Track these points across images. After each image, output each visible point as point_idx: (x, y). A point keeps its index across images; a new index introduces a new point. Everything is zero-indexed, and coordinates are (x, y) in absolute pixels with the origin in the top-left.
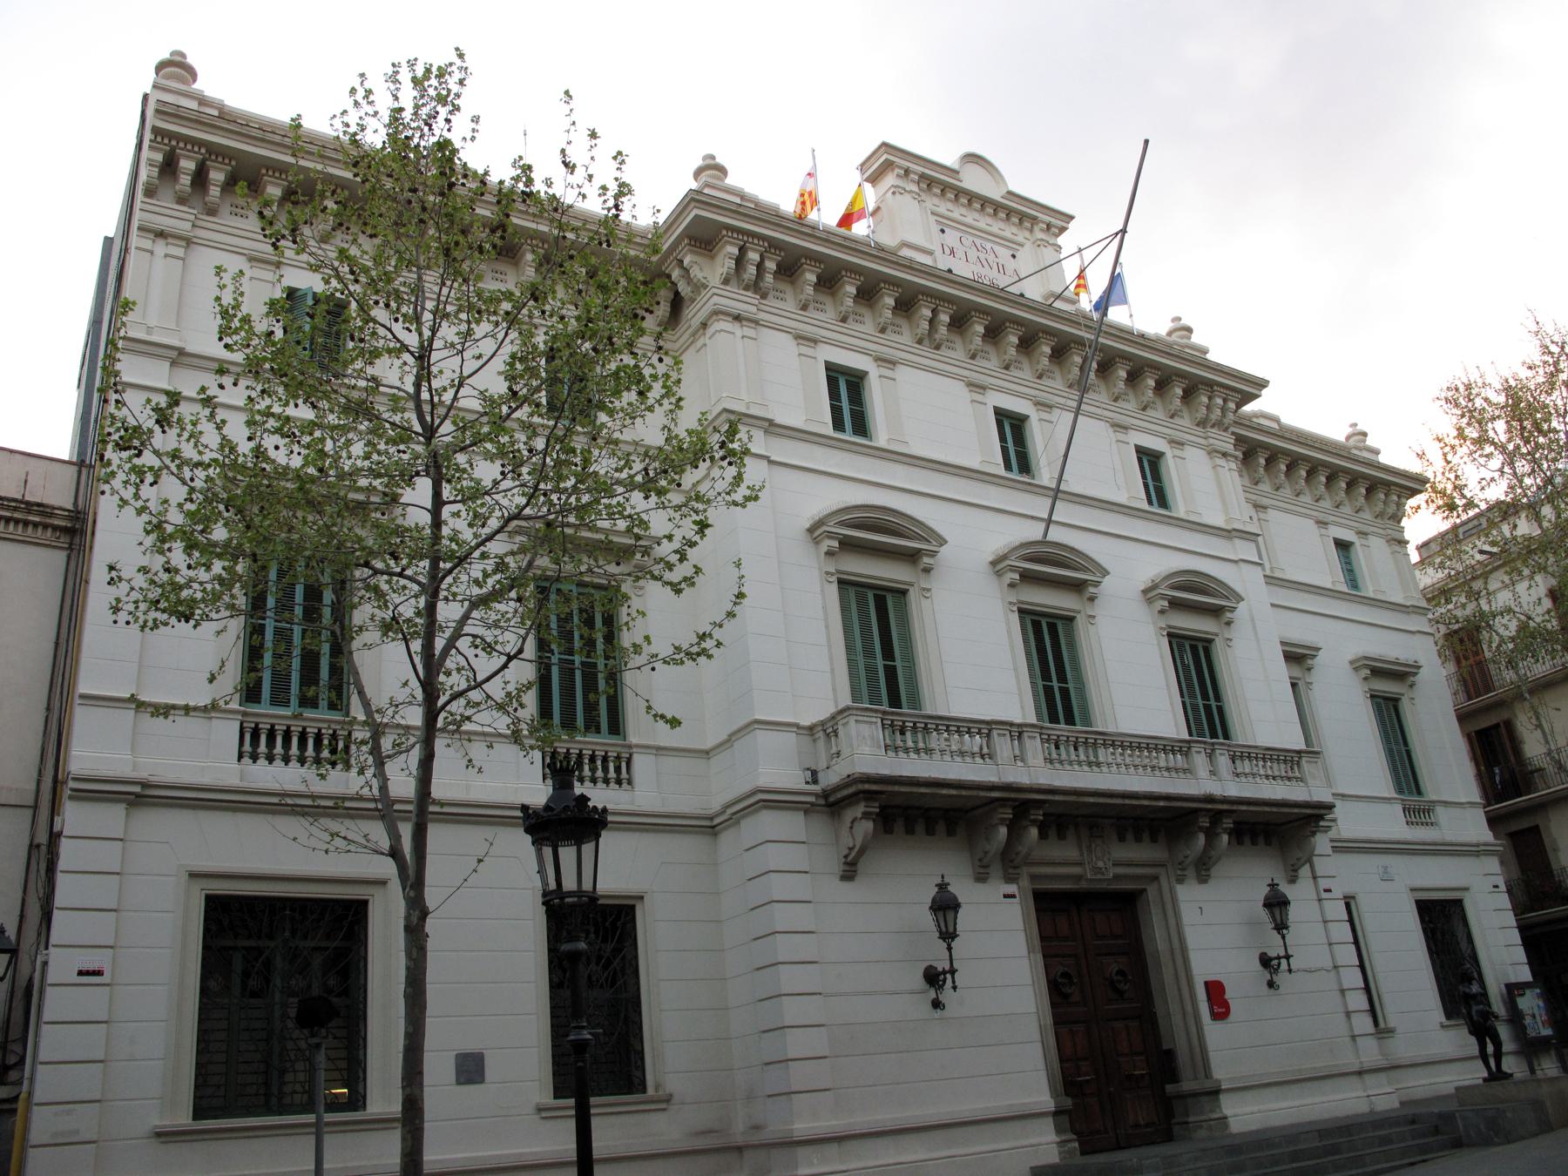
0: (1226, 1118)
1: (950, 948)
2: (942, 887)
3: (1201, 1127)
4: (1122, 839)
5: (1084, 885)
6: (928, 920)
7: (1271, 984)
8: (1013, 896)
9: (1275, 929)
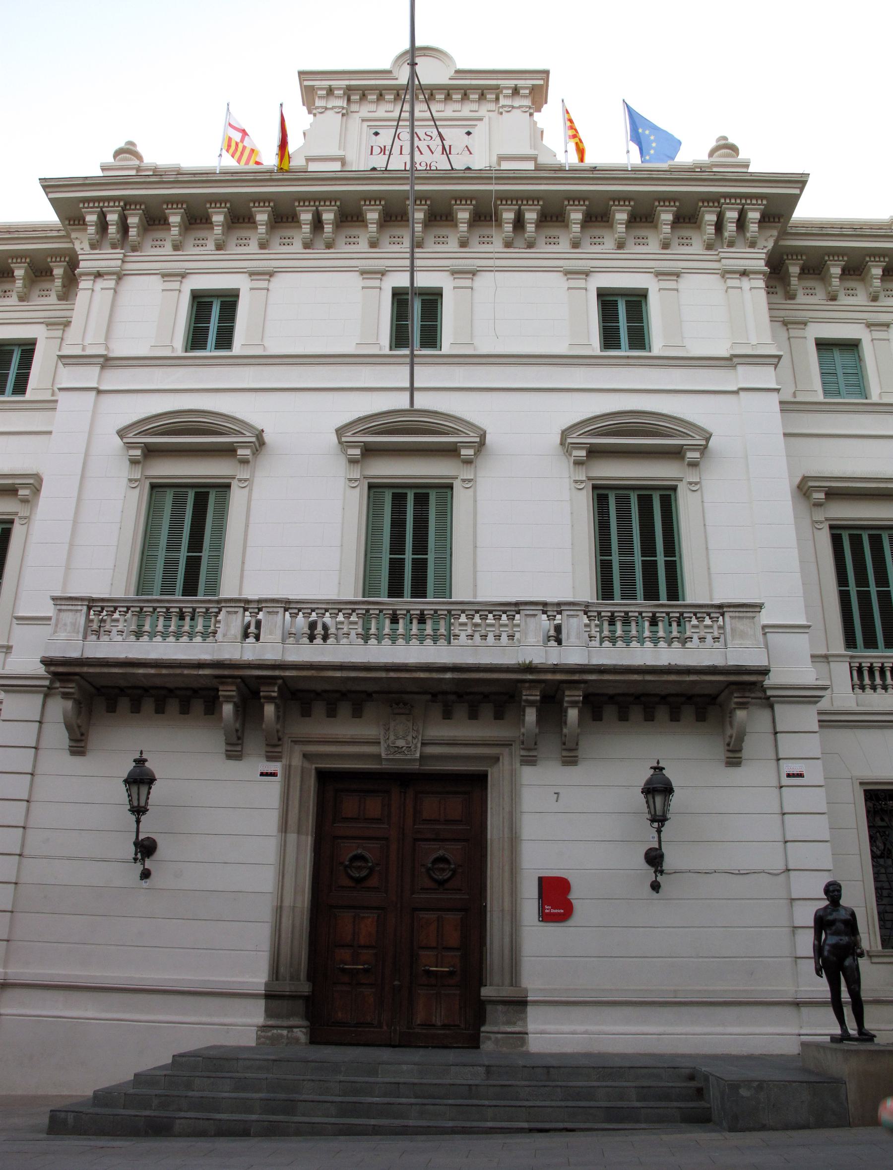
0: (527, 1034)
1: (138, 822)
2: (140, 762)
3: (489, 1038)
4: (447, 715)
5: (385, 766)
7: (656, 887)
8: (274, 775)
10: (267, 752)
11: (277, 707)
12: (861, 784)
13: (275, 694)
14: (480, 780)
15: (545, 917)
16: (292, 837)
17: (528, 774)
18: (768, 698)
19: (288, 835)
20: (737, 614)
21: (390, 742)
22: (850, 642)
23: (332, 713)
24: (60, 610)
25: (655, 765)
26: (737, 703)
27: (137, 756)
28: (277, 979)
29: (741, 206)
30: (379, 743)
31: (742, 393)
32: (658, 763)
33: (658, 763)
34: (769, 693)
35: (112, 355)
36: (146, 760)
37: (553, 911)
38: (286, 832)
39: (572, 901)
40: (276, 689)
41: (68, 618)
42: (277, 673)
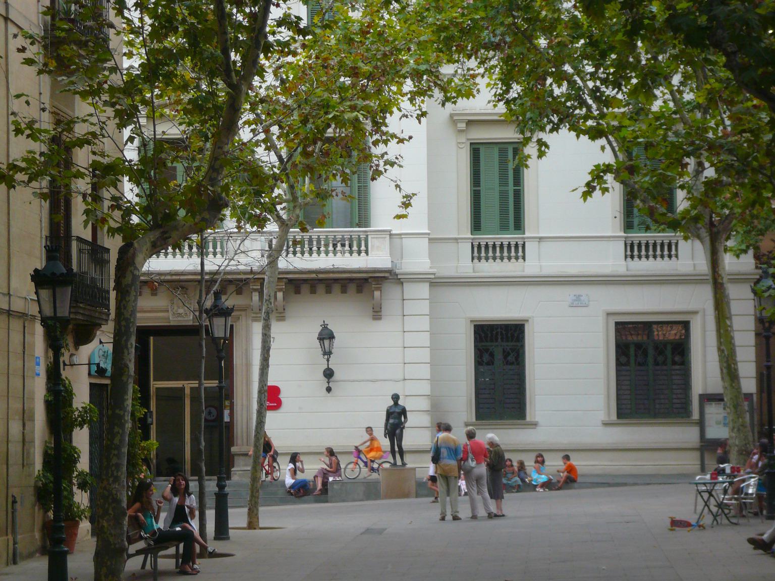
3: (236, 474)
7: (329, 390)
12: (471, 321)
18: (400, 279)
20: (376, 236)
21: (174, 310)
22: (476, 226)
26: (374, 287)
34: (399, 277)
37: (270, 404)
39: (282, 399)
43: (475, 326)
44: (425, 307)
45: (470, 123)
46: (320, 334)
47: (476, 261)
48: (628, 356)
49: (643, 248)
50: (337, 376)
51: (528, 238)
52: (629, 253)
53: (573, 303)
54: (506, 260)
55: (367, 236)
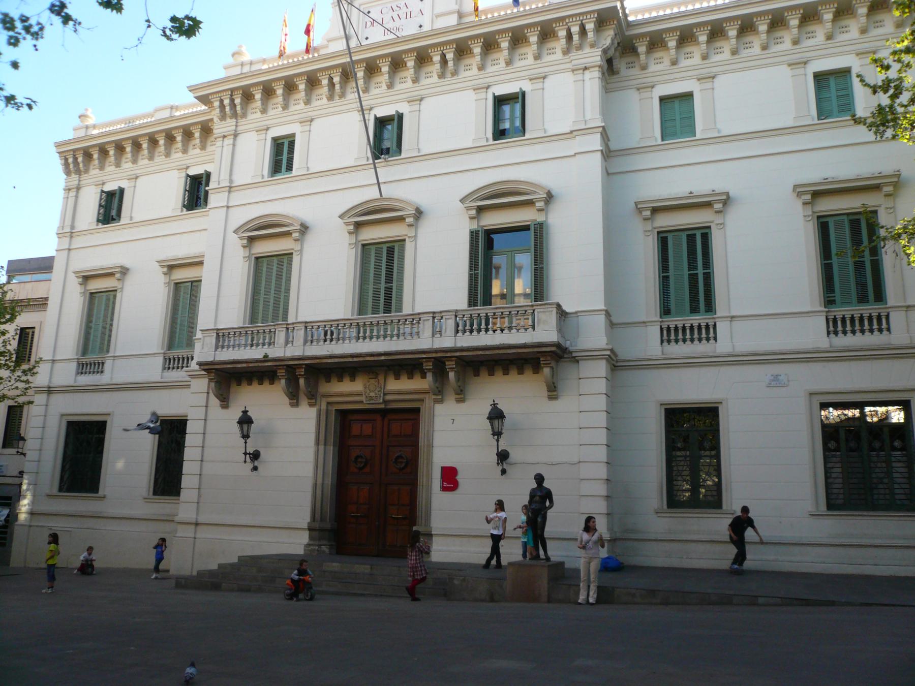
1: (246, 443)
2: (245, 412)
4: (397, 377)
6: (236, 428)
7: (504, 472)
9: (492, 434)
10: (309, 403)
11: (306, 379)
12: (661, 404)
13: (303, 373)
14: (417, 411)
15: (444, 489)
16: (322, 447)
17: (439, 408)
18: (574, 357)
19: (320, 446)
20: (542, 310)
22: (666, 311)
23: (340, 379)
24: (204, 336)
25: (493, 403)
26: (544, 364)
27: (244, 409)
28: (314, 521)
29: (580, 22)
30: (362, 395)
31: (577, 156)
32: (494, 401)
33: (494, 401)
34: (574, 354)
35: (233, 185)
36: (248, 411)
37: (447, 485)
38: (318, 445)
39: (459, 480)
40: (303, 370)
41: (208, 340)
42: (301, 362)
43: (666, 409)
44: (601, 386)
45: (655, 210)
46: (490, 413)
47: (665, 344)
48: (837, 441)
49: (848, 322)
50: (514, 456)
51: (719, 318)
52: (831, 329)
53: (770, 384)
54: (696, 342)
55: (534, 311)
